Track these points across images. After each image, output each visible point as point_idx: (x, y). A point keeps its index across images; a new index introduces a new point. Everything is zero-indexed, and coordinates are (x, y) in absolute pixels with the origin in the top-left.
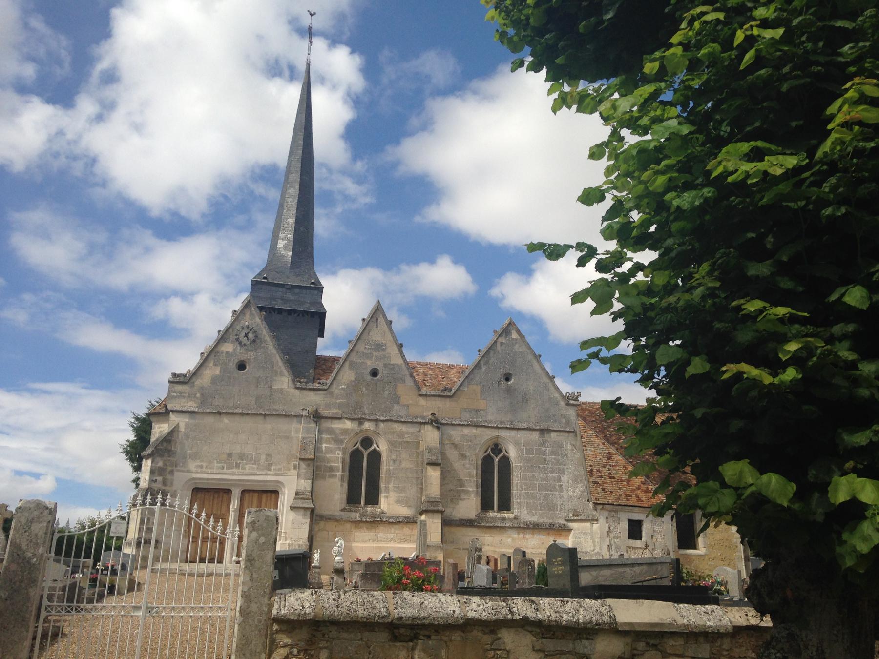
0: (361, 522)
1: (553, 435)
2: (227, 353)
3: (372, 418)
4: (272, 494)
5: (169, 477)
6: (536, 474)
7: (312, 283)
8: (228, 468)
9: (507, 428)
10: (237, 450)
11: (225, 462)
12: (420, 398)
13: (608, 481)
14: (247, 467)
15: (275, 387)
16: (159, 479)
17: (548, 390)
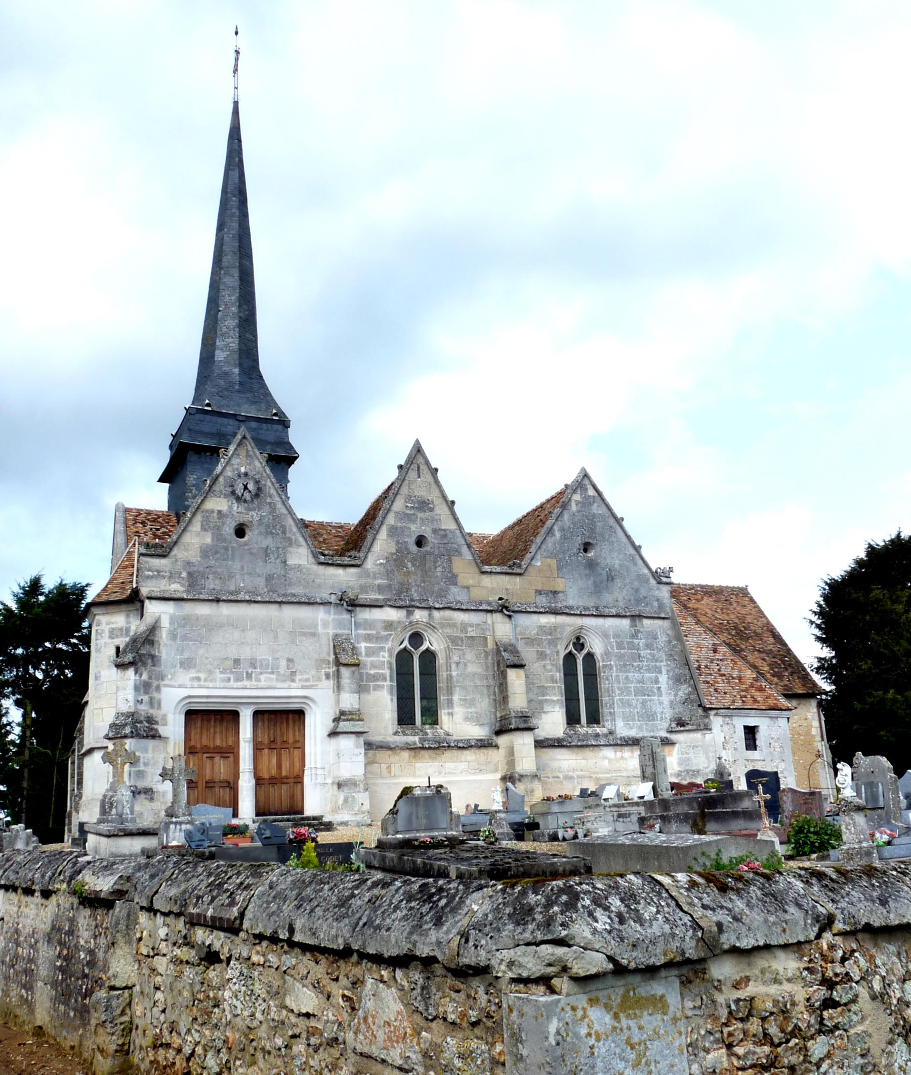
0: (423, 748)
1: (646, 622)
2: (220, 512)
3: (423, 605)
4: (295, 716)
5: (156, 695)
6: (630, 675)
7: (275, 415)
8: (237, 680)
9: (593, 615)
10: (246, 653)
11: (232, 672)
12: (484, 577)
13: (719, 679)
14: (263, 677)
15: (290, 562)
16: (146, 698)
17: (635, 564)
